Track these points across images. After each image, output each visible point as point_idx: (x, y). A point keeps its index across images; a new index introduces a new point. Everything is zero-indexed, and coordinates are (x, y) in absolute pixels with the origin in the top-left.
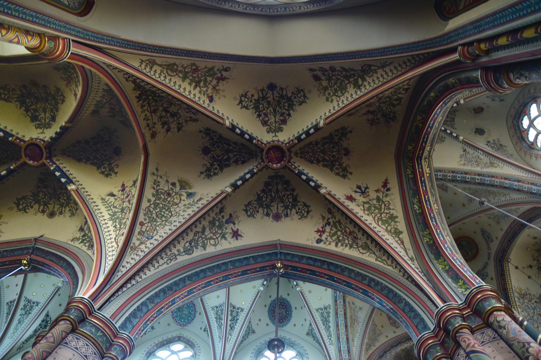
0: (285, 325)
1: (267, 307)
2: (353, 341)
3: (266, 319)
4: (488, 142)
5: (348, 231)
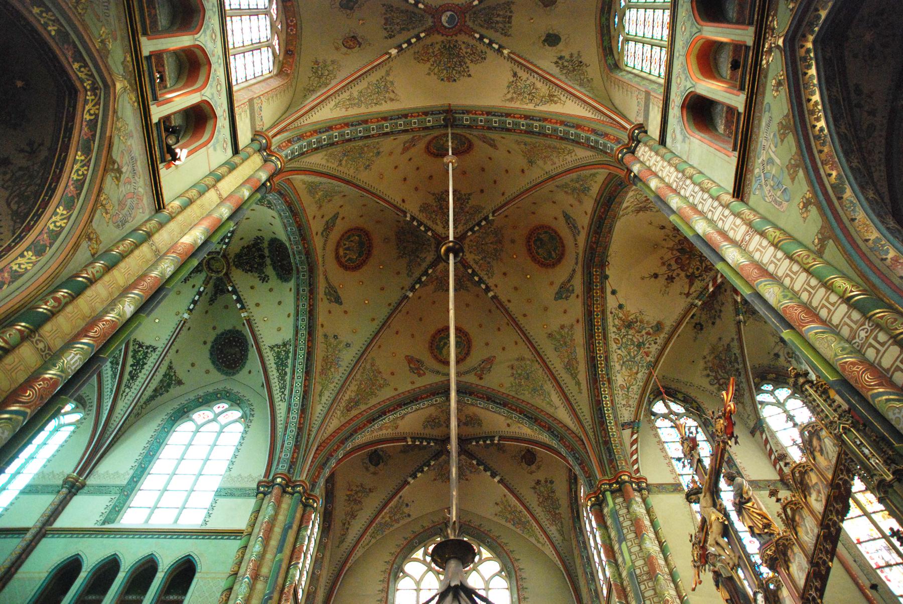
0: (238, 372)
1: (209, 345)
2: (320, 396)
3: (204, 360)
4: (561, 58)
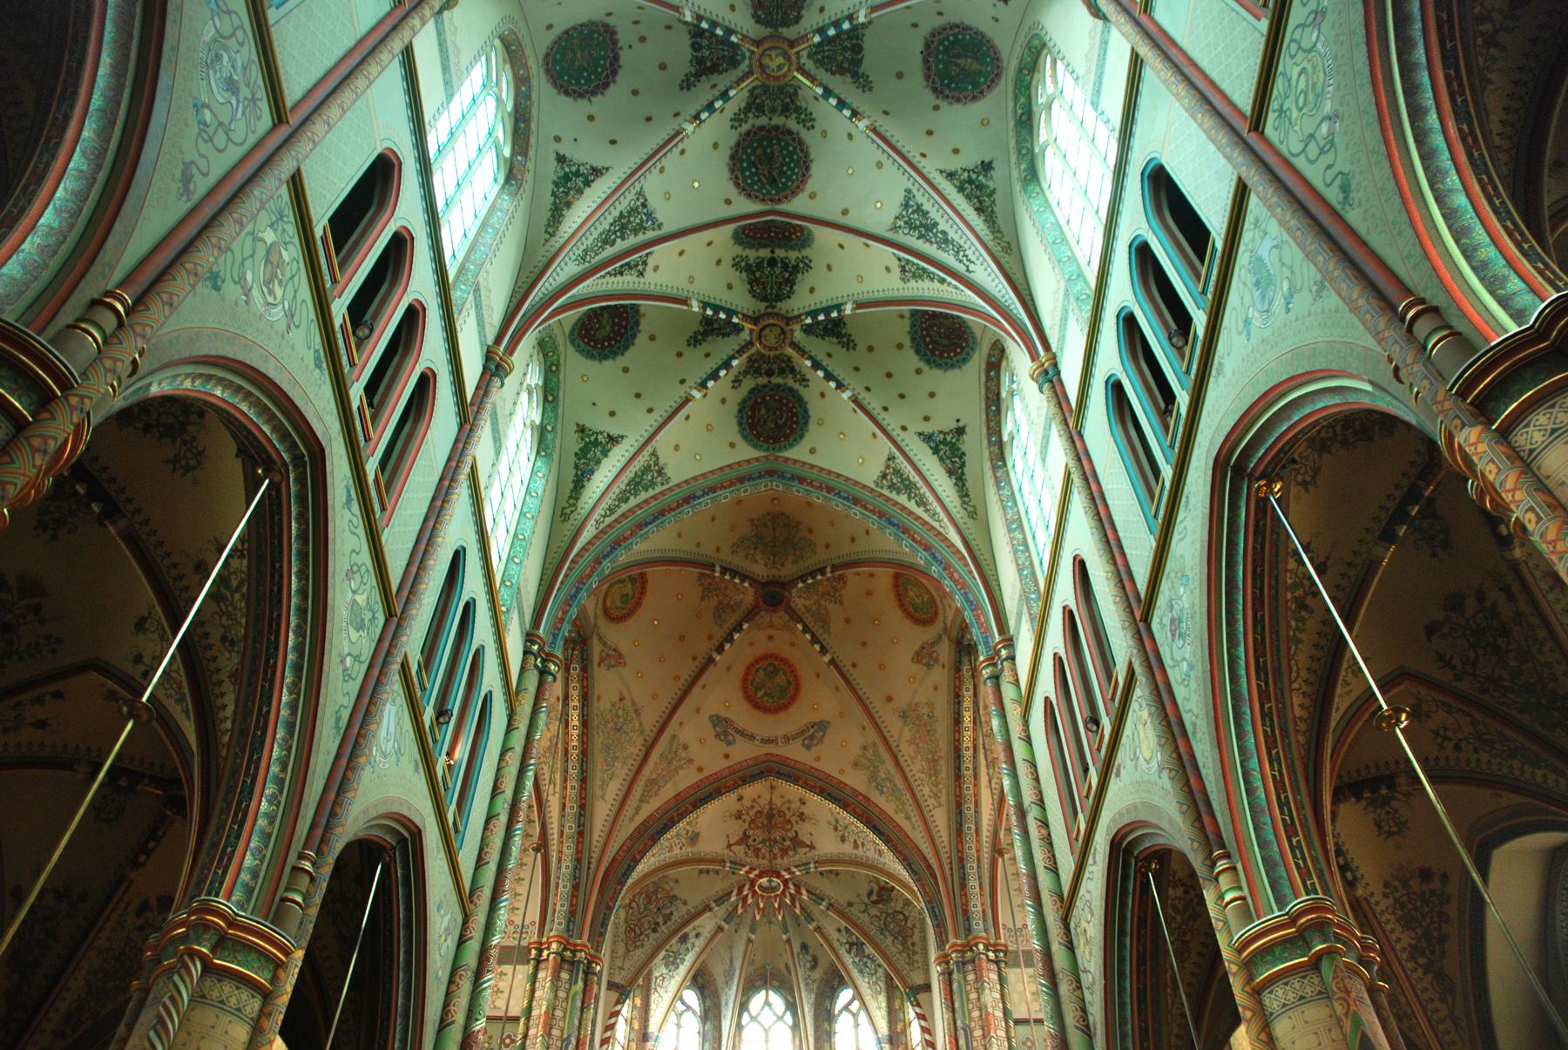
5: (1188, 938)
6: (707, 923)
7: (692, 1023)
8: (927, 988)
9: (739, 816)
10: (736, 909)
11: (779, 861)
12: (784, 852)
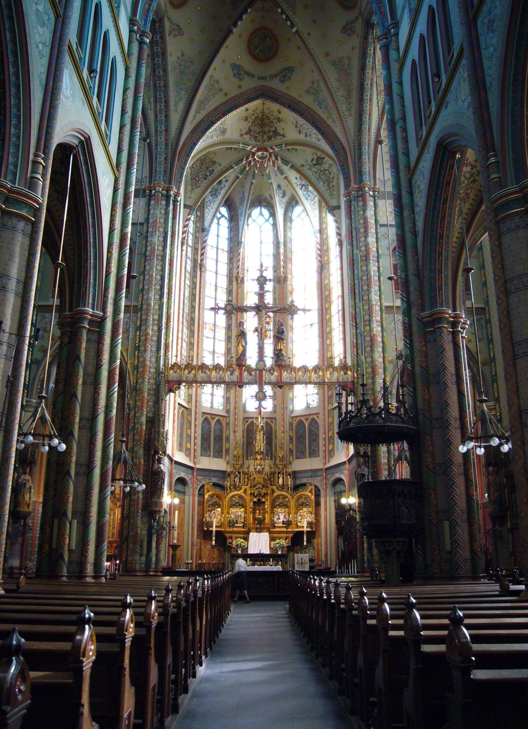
5: (469, 191)
6: (230, 174)
7: (224, 223)
8: (339, 207)
9: (246, 119)
10: (245, 168)
11: (267, 143)
12: (270, 138)
